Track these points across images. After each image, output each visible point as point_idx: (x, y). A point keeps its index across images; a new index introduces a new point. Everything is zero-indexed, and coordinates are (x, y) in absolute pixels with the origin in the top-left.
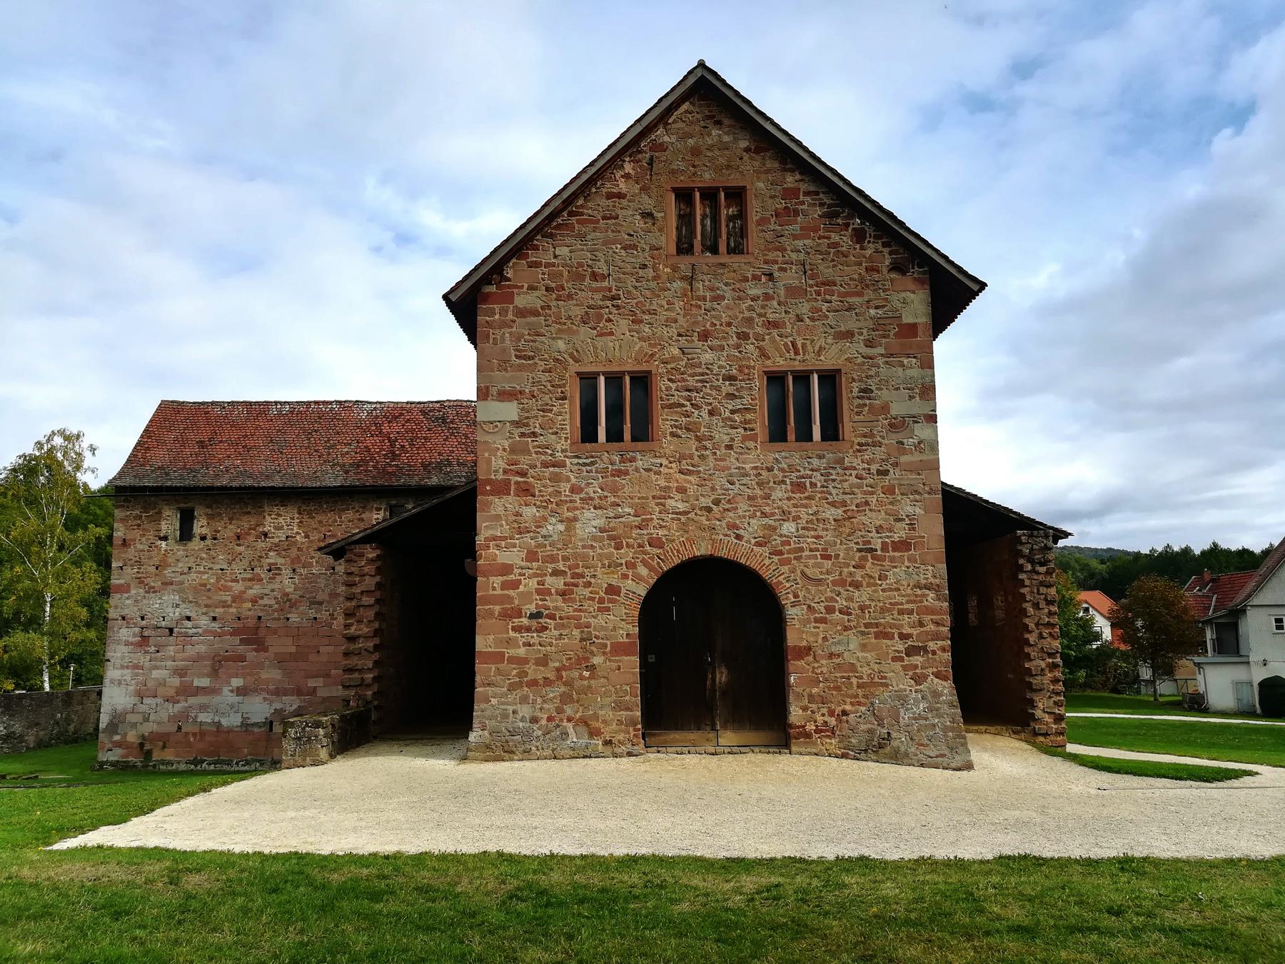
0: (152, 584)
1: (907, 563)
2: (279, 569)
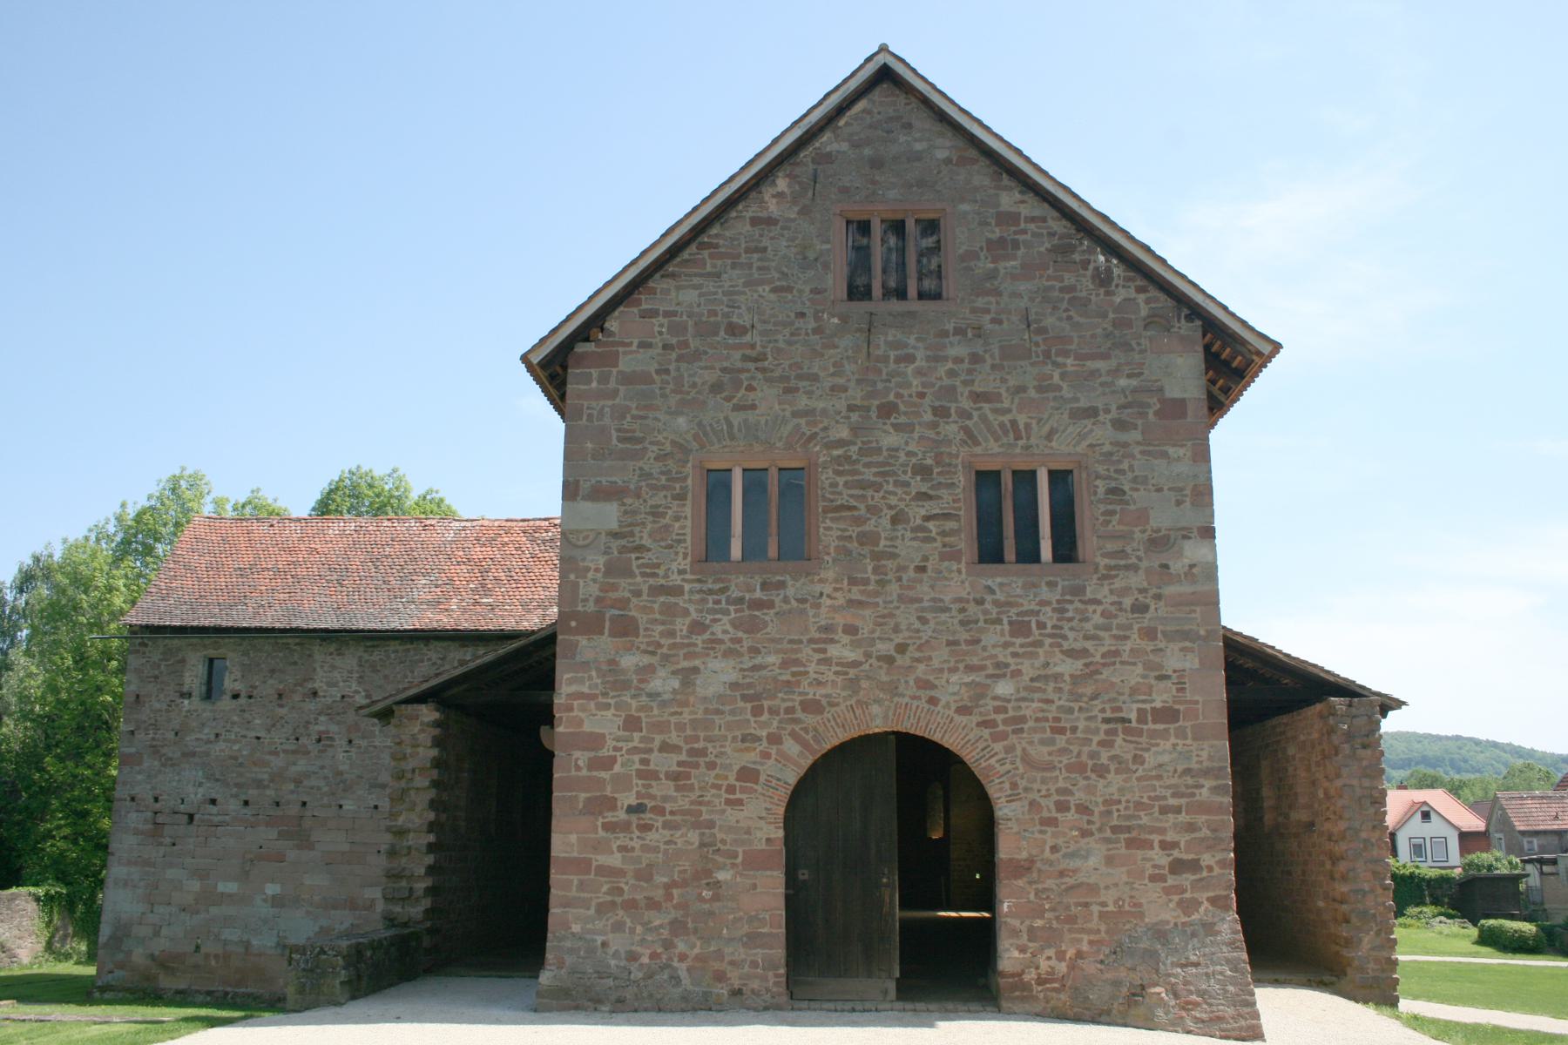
0: (170, 755)
1: (1173, 740)
2: (331, 739)
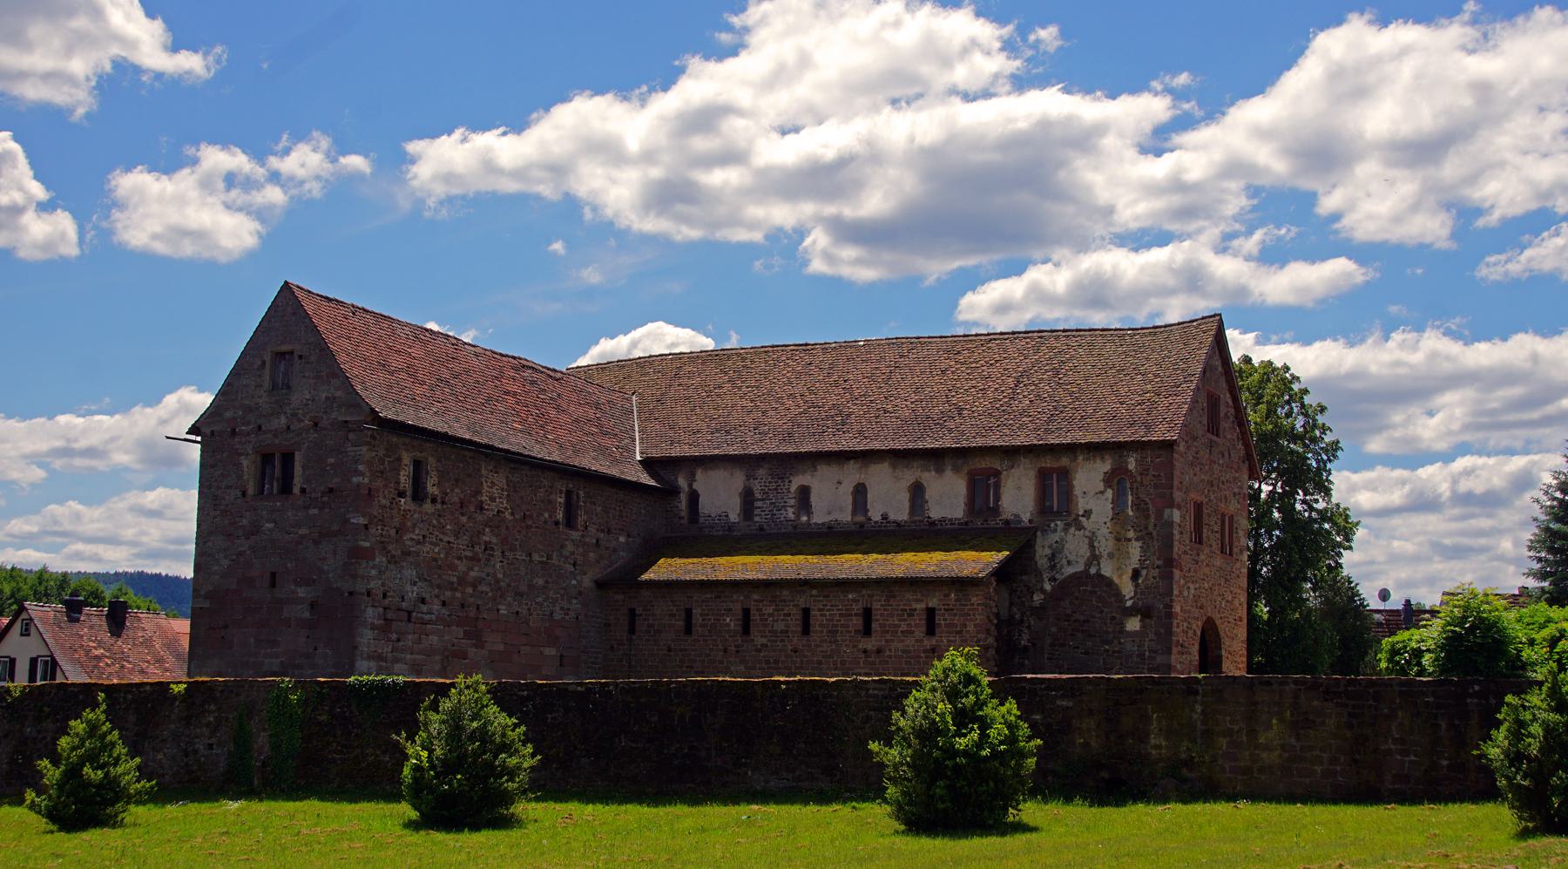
0: (394, 552)
